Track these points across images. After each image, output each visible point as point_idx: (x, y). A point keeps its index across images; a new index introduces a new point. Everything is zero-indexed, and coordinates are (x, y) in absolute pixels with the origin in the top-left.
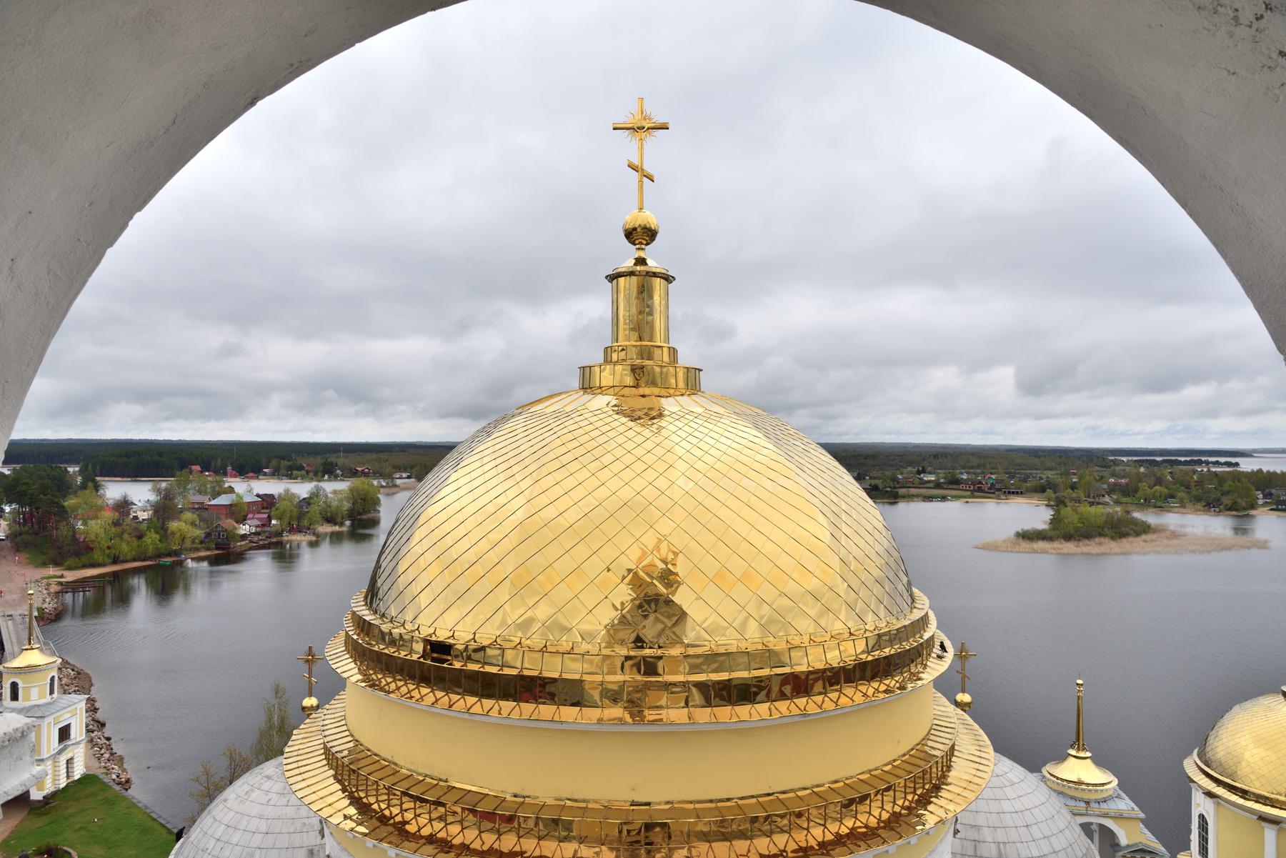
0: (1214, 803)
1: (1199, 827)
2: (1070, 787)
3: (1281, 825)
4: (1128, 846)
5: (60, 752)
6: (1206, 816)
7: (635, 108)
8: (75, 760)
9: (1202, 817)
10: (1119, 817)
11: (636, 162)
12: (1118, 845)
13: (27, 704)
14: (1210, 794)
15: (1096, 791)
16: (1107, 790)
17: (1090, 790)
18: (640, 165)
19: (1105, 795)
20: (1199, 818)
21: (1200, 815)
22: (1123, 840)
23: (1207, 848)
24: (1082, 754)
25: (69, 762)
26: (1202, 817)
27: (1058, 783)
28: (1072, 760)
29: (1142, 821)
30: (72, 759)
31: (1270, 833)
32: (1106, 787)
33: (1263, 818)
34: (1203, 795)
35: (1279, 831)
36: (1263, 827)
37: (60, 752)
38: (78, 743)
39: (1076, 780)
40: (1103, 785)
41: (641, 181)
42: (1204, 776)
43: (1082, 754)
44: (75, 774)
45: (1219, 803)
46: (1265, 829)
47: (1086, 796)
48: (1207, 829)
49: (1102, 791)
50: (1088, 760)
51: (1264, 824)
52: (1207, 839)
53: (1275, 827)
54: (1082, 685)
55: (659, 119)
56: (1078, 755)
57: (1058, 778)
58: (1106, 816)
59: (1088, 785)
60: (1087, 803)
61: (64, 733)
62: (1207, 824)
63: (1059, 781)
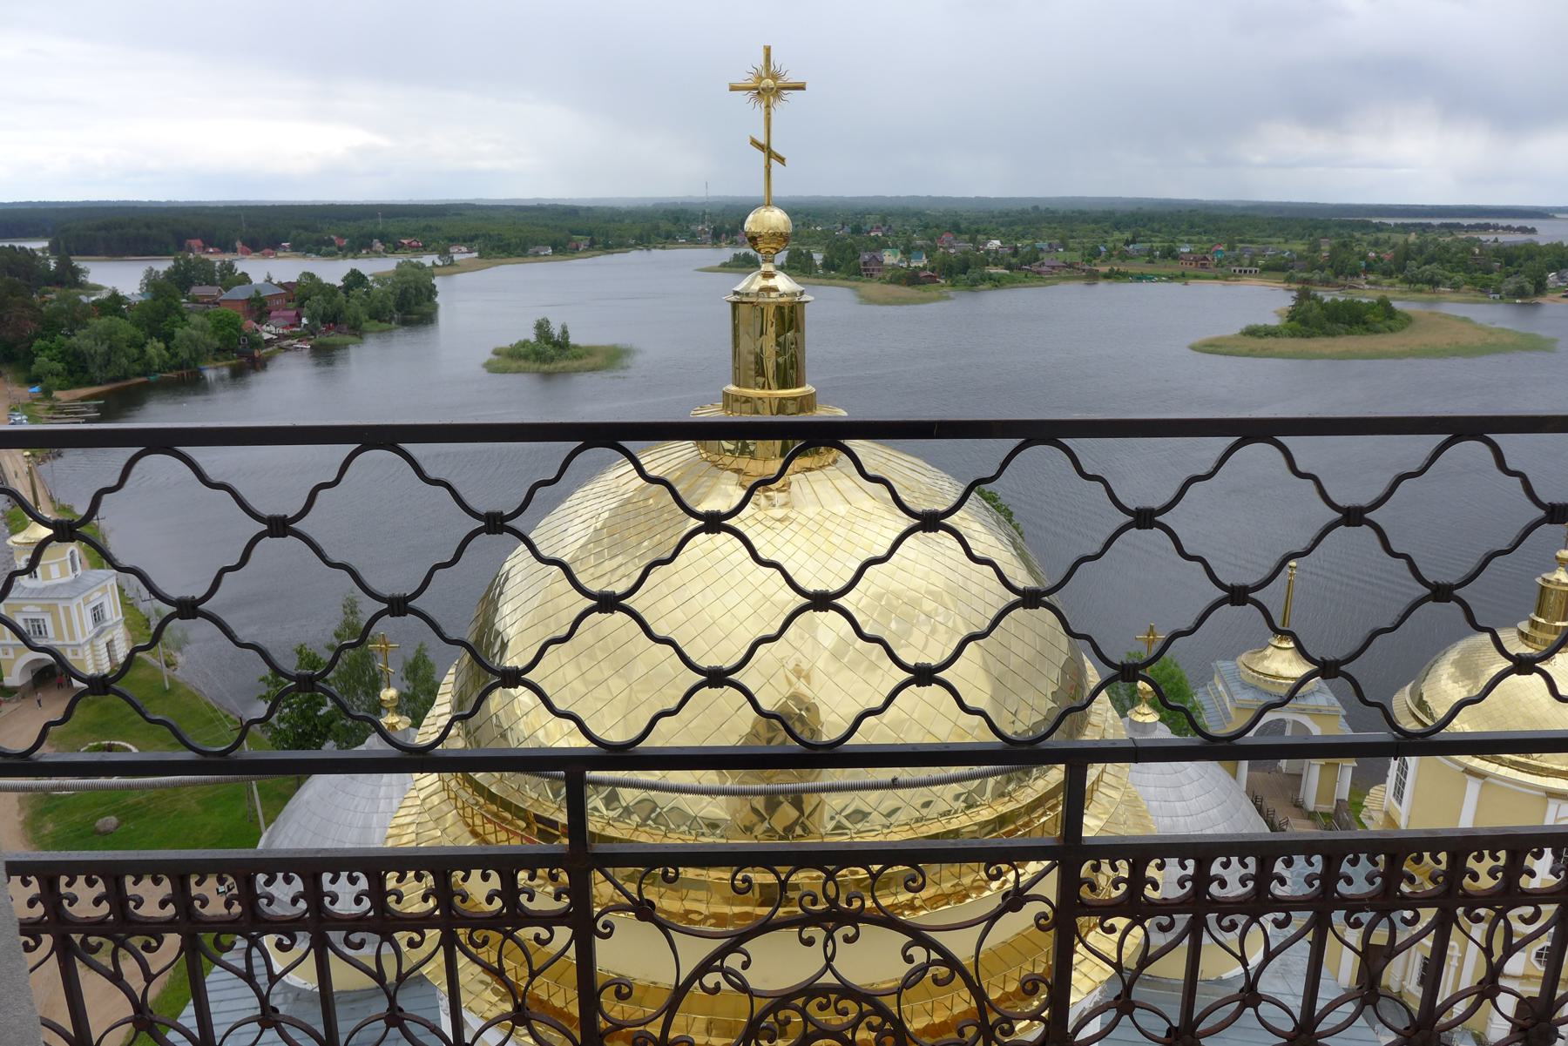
2: (1265, 681)
3: (1487, 779)
5: (97, 635)
7: (760, 61)
8: (116, 642)
11: (762, 140)
13: (47, 583)
18: (766, 143)
25: (109, 645)
27: (1253, 677)
28: (1273, 648)
29: (1343, 716)
30: (112, 641)
31: (1473, 787)
36: (1467, 780)
37: (97, 635)
38: (116, 624)
39: (1274, 674)
42: (1412, 719)
43: (1285, 645)
44: (118, 657)
48: (1406, 773)
50: (1289, 652)
51: (1467, 777)
52: (1404, 784)
53: (1480, 781)
54: (1295, 568)
55: (792, 78)
56: (1279, 645)
57: (1254, 671)
58: (1302, 711)
61: (98, 615)
62: (1407, 768)
63: (1255, 674)
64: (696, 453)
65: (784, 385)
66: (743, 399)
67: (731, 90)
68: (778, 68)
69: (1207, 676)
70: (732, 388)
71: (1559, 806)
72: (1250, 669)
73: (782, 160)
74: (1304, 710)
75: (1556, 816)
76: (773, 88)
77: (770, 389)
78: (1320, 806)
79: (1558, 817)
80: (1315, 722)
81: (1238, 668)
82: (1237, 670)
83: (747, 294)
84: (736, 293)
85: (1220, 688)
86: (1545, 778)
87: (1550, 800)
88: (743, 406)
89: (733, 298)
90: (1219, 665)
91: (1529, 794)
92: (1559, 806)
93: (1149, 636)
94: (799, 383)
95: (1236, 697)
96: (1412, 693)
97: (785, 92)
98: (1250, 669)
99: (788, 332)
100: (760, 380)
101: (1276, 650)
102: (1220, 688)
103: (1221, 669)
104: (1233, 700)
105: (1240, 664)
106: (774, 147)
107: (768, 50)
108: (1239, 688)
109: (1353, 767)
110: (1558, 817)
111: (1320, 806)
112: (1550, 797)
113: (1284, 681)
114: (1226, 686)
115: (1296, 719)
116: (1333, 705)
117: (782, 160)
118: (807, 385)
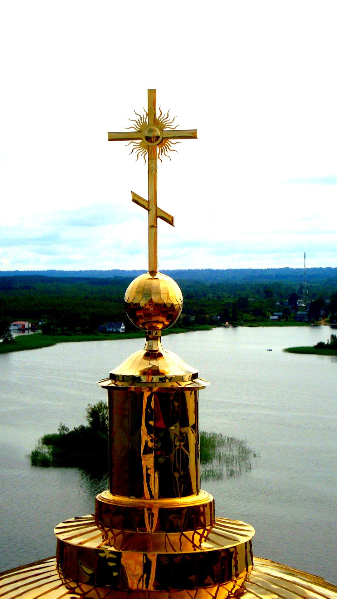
41: (153, 227)
55: (182, 125)
64: (60, 582)
65: (166, 492)
67: (110, 140)
68: (165, 113)
73: (170, 221)
76: (158, 138)
77: (152, 497)
83: (124, 378)
84: (113, 377)
89: (109, 383)
94: (188, 492)
97: (173, 141)
99: (171, 425)
106: (162, 204)
107: (152, 94)
117: (170, 221)
118: (202, 491)
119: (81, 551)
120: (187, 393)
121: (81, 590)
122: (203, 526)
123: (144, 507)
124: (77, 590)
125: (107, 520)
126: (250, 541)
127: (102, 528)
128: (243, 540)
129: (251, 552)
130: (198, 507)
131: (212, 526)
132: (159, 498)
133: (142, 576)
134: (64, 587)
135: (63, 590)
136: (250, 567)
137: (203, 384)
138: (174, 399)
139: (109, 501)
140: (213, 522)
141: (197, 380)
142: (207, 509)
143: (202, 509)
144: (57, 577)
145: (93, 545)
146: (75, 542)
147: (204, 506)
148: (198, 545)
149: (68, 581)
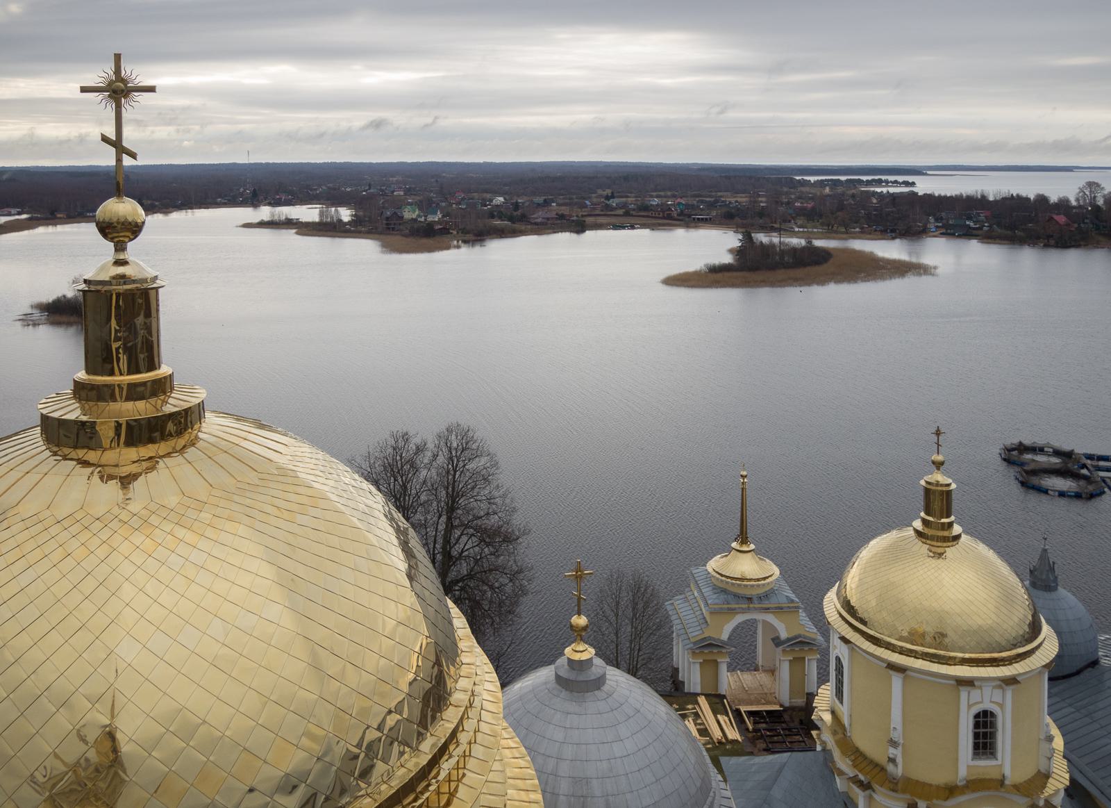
0: (849, 649)
1: (836, 670)
2: (733, 584)
3: (908, 672)
4: (789, 640)
6: (842, 659)
9: (838, 659)
10: (779, 610)
12: (778, 638)
14: (845, 640)
15: (758, 586)
16: (768, 583)
17: (752, 586)
19: (767, 589)
20: (836, 660)
21: (837, 657)
22: (784, 635)
23: (842, 683)
24: (745, 548)
26: (838, 659)
27: (722, 581)
32: (768, 581)
33: (892, 667)
34: (839, 640)
35: (904, 679)
36: (891, 676)
39: (740, 577)
40: (765, 579)
45: (853, 648)
46: (893, 677)
47: (748, 593)
49: (764, 585)
51: (891, 672)
53: (901, 675)
57: (722, 575)
59: (750, 580)
60: (750, 599)
63: (723, 578)
64: (44, 447)
66: (89, 387)
69: (682, 585)
70: (82, 375)
71: (969, 693)
72: (719, 574)
74: (768, 609)
75: (968, 703)
77: (121, 374)
78: (793, 700)
79: (970, 703)
80: (776, 617)
81: (709, 573)
82: (709, 576)
85: (696, 594)
86: (953, 667)
87: (961, 688)
88: (89, 393)
90: (694, 572)
91: (940, 683)
92: (969, 693)
93: (577, 572)
95: (709, 602)
96: (838, 594)
98: (719, 574)
100: (108, 366)
101: (738, 553)
102: (696, 594)
103: (695, 575)
104: (707, 604)
105: (710, 570)
108: (711, 593)
109: (818, 659)
110: (970, 703)
111: (793, 700)
112: (962, 685)
113: (748, 583)
114: (700, 591)
115: (764, 618)
116: (792, 601)
119: (62, 423)
120: (150, 291)
121: (63, 453)
122: (165, 393)
123: (114, 385)
124: (59, 453)
125: (83, 394)
126: (203, 401)
127: (79, 402)
128: (197, 401)
129: (203, 409)
130: (161, 379)
131: (171, 392)
132: (127, 375)
133: (114, 438)
134: (48, 450)
135: (48, 453)
136: (202, 421)
137: (163, 284)
138: (139, 298)
139: (85, 380)
140: (172, 389)
141: (157, 281)
142: (169, 380)
143: (163, 380)
144: (42, 443)
145: (71, 416)
146: (56, 415)
147: (165, 378)
148: (160, 409)
149: (51, 446)
